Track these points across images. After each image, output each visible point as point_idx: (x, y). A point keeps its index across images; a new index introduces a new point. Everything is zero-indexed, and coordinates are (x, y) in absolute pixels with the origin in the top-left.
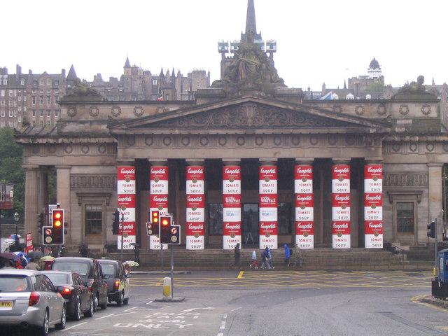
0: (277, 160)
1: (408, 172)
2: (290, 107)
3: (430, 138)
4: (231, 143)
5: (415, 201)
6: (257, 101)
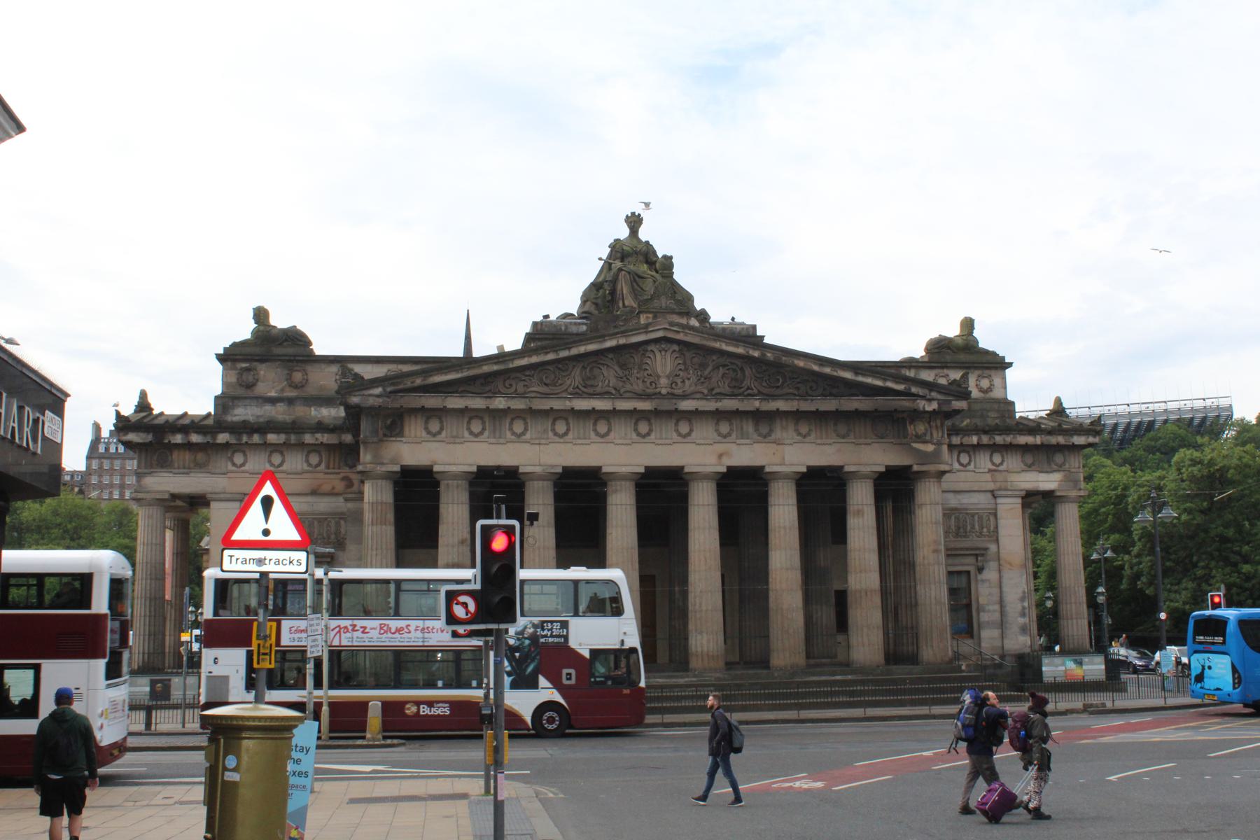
0: (725, 470)
1: (956, 509)
3: (999, 439)
4: (622, 430)
5: (972, 569)
6: (681, 337)
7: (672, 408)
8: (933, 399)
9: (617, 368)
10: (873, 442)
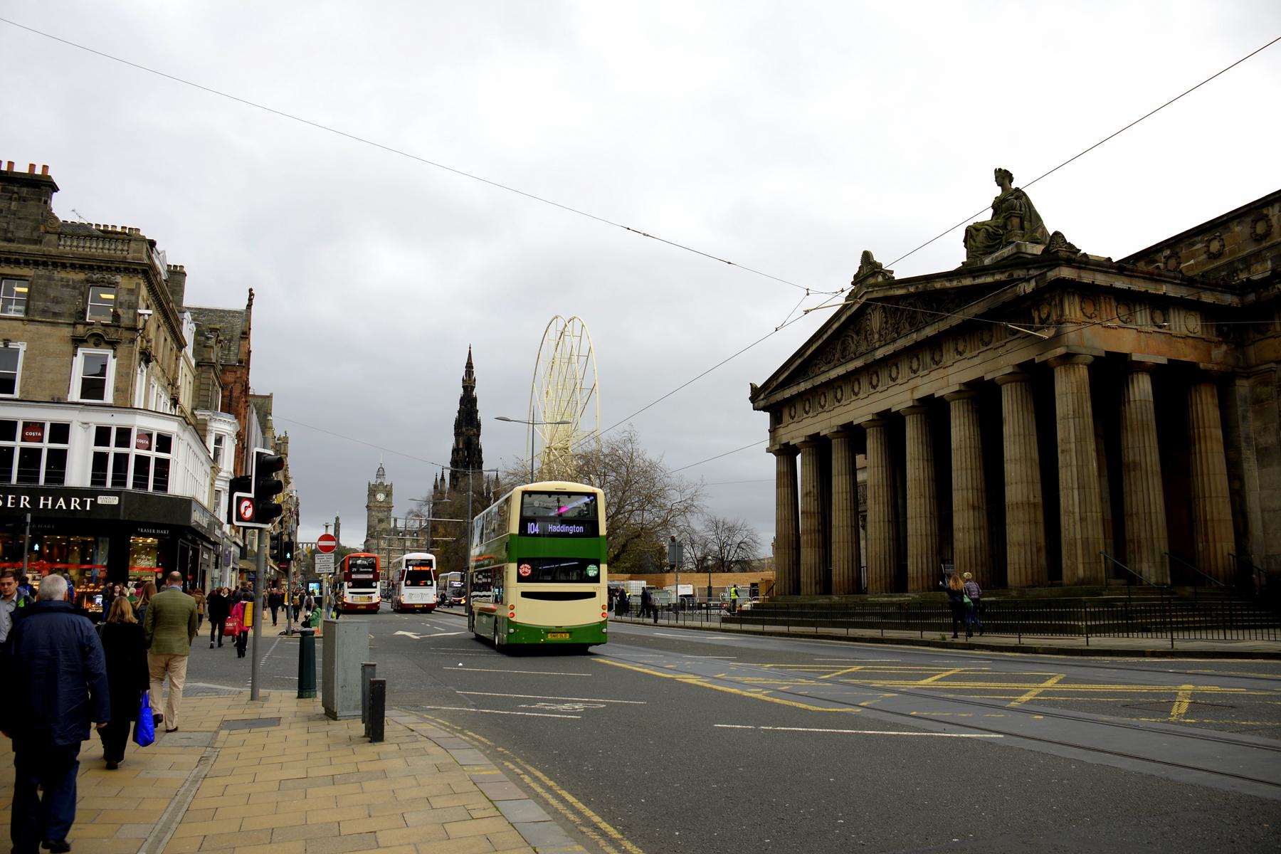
2: (912, 289)
6: (875, 295)
7: (872, 360)
8: (1031, 278)
9: (855, 336)
10: (1006, 343)
